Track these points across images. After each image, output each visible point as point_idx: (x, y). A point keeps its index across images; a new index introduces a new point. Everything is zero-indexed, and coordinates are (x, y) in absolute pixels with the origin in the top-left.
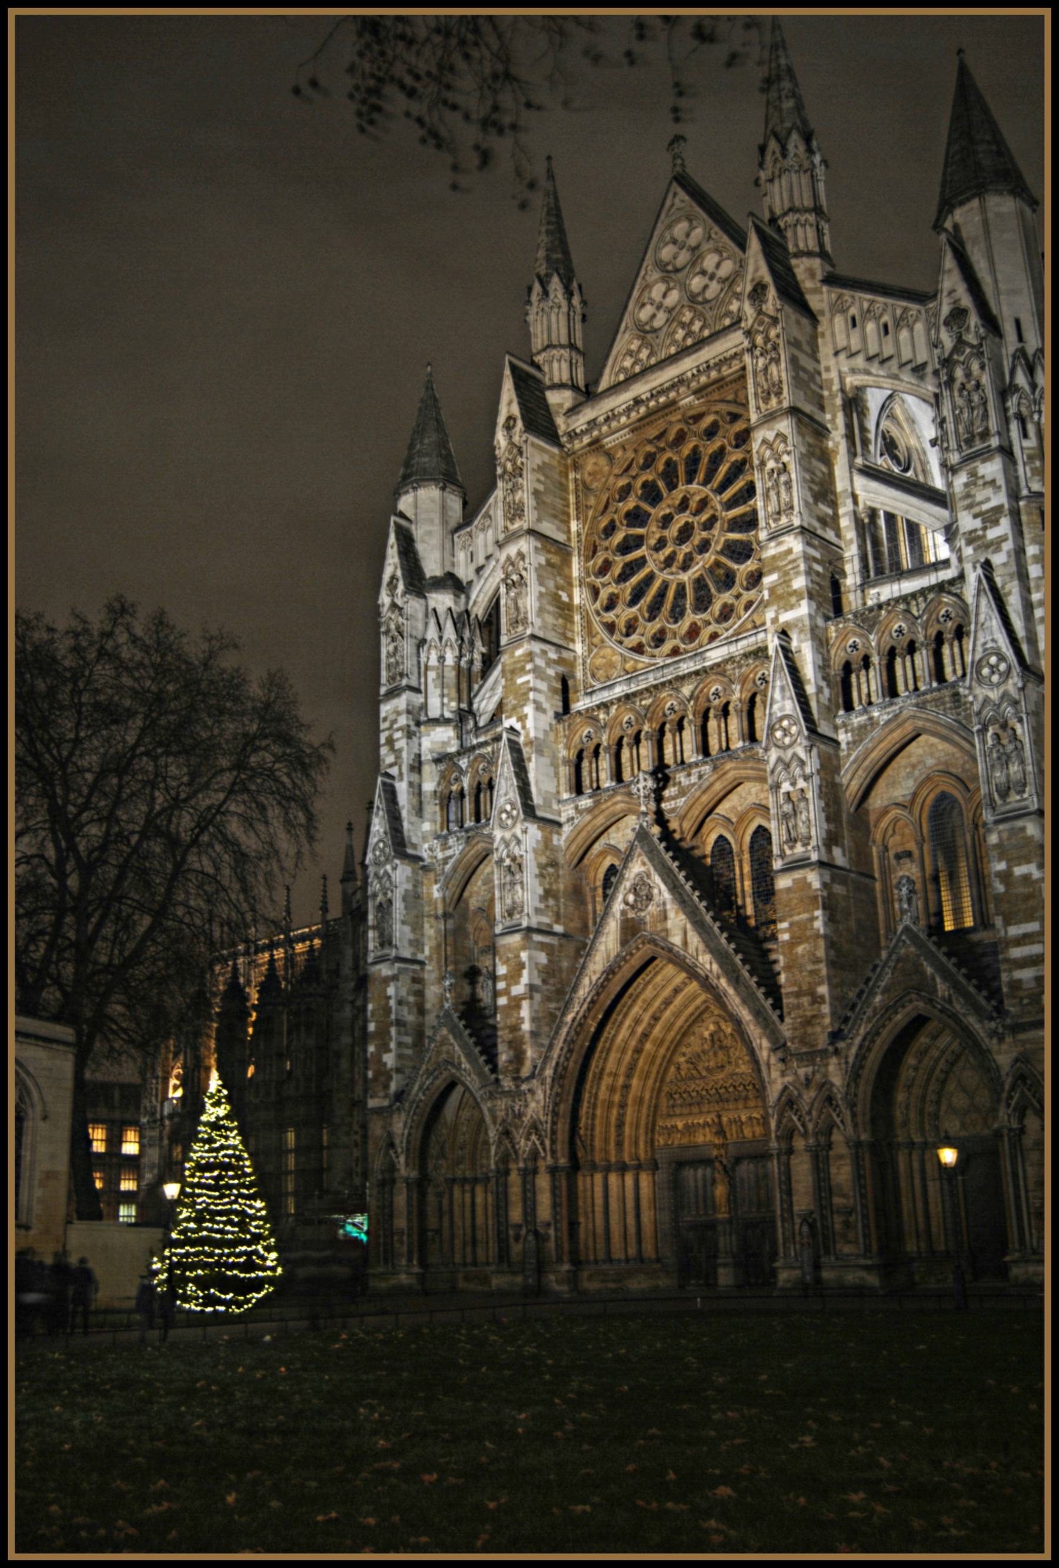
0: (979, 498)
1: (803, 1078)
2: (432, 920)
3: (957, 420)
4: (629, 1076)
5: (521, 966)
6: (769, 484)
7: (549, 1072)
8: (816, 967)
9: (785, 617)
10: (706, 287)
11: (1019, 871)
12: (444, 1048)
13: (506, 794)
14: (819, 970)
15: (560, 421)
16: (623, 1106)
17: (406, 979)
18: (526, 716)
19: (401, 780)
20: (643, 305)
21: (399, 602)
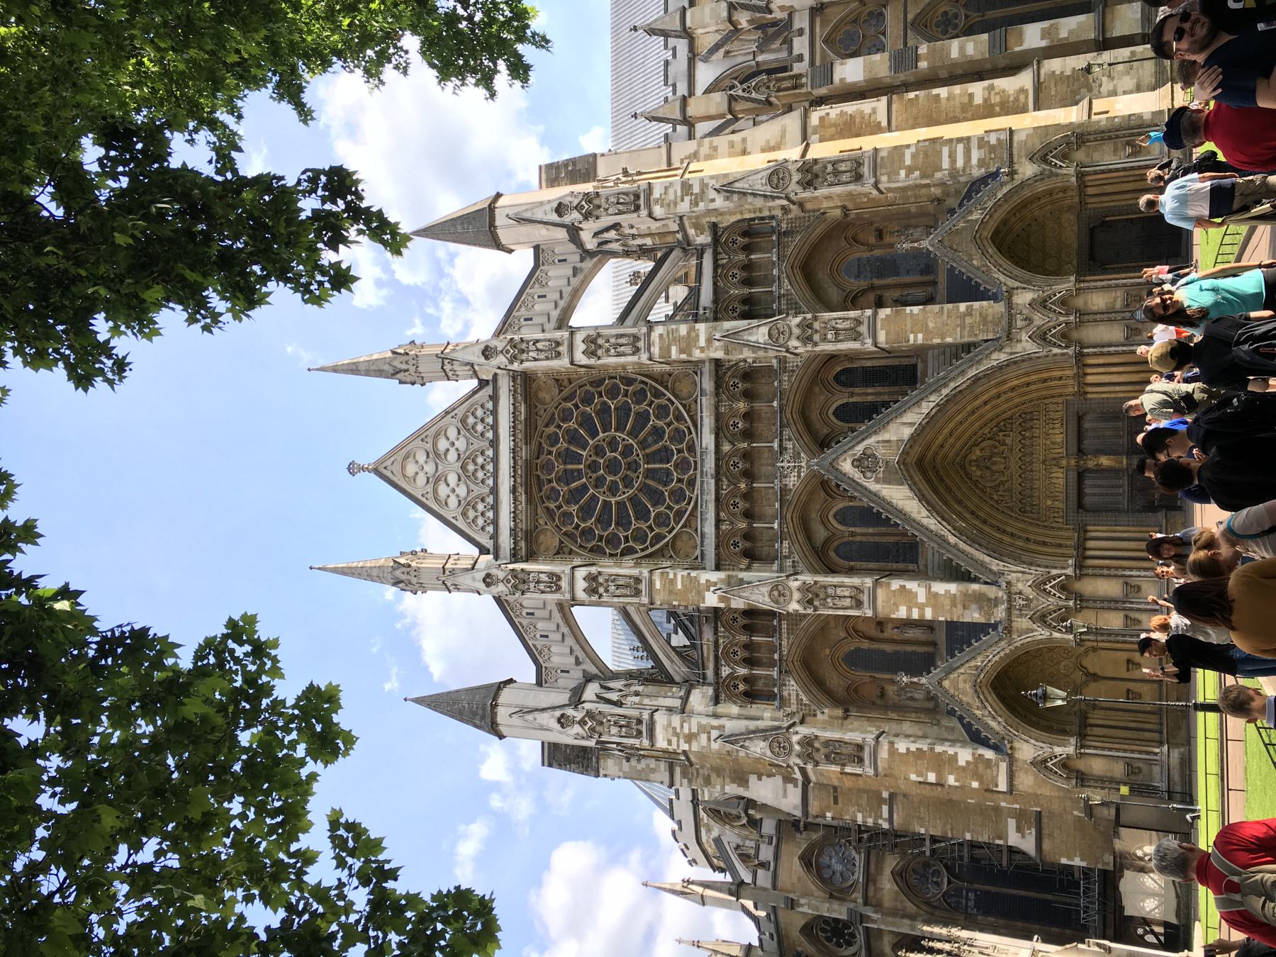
0: (671, 196)
1: (1024, 323)
2: (845, 722)
3: (620, 213)
4: (1004, 532)
6: (613, 351)
7: (995, 565)
8: (946, 311)
9: (702, 343)
10: (457, 450)
11: (908, 161)
12: (961, 685)
17: (896, 740)
18: (708, 581)
20: (446, 503)
21: (579, 715)
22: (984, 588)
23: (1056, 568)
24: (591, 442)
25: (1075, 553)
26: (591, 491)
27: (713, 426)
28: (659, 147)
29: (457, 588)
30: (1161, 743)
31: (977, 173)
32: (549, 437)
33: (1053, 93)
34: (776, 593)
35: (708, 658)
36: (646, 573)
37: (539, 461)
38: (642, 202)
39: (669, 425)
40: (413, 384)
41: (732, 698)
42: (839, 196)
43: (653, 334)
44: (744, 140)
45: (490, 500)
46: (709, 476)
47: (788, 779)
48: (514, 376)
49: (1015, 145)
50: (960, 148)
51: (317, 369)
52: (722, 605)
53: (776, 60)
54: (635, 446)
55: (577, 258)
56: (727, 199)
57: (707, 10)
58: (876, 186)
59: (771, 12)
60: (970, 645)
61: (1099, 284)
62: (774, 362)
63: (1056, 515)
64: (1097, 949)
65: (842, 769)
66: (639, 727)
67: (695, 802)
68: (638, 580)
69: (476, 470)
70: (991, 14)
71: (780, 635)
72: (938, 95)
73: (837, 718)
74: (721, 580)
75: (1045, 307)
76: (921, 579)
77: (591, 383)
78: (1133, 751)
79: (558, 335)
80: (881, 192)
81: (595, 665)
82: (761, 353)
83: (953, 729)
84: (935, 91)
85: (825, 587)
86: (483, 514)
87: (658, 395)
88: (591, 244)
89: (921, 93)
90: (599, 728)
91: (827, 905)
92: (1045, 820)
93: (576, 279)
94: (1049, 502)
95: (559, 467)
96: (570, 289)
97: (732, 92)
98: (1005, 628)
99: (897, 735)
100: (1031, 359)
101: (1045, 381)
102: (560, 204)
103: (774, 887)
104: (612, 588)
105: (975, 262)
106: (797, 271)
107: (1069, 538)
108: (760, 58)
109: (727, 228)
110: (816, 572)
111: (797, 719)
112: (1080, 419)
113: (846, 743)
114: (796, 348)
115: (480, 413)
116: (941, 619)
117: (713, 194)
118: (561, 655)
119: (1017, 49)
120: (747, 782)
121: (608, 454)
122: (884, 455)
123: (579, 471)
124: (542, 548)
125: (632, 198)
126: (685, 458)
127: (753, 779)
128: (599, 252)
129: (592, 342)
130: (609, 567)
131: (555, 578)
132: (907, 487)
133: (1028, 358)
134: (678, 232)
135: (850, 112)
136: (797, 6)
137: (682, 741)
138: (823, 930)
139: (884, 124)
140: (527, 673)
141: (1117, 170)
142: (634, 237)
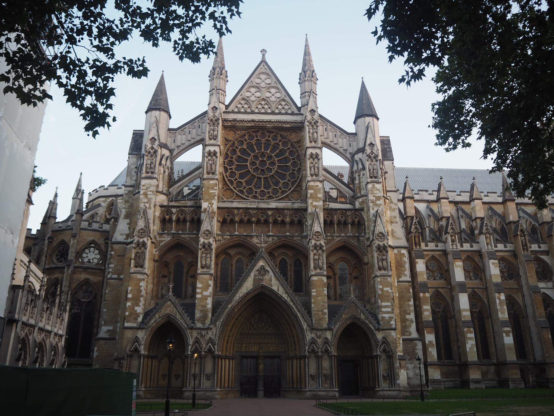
0: (376, 192)
1: (318, 335)
2: (152, 261)
3: (370, 170)
5: (210, 286)
6: (312, 165)
7: (219, 323)
9: (315, 203)
11: (385, 289)
12: (168, 309)
13: (207, 227)
14: (325, 305)
15: (222, 114)
16: (229, 336)
17: (145, 282)
18: (213, 204)
19: (150, 209)
20: (248, 91)
21: (155, 146)
22: (209, 319)
23: (218, 347)
24: (273, 155)
25: (224, 355)
26: (252, 154)
27: (279, 207)
28: (395, 187)
29: (210, 95)
30: (145, 388)
31: (380, 316)
32: (276, 136)
33: (409, 346)
34: (207, 233)
35: (179, 203)
36: (217, 177)
37: (265, 132)
38: (374, 179)
39: (280, 188)
40: (300, 79)
41: (162, 212)
42: (373, 261)
43: (319, 182)
44: (397, 223)
45: (249, 110)
46: (258, 205)
47: (128, 236)
48: (302, 123)
49: (390, 331)
50: (390, 310)
51: (306, 38)
52: (202, 209)
53: (426, 236)
54: (271, 174)
55: (351, 152)
56: (374, 215)
57: (447, 208)
58: (376, 276)
59: (445, 234)
60: (186, 312)
61: (333, 364)
62: (305, 234)
63: (239, 347)
64: (63, 360)
65: (133, 259)
66: (150, 173)
67: (117, 196)
68: (213, 173)
69: (262, 105)
70: (439, 321)
71: (190, 234)
72: (410, 301)
73: (154, 257)
74: (213, 210)
75: (325, 343)
76: (213, 293)
77: (298, 155)
78: (142, 376)
79: (319, 142)
80: (374, 278)
81: (177, 154)
82: (309, 228)
83: (150, 305)
84: (412, 300)
85: (210, 253)
86: (243, 107)
87: (293, 184)
88: (357, 157)
89: (411, 294)
90: (149, 155)
91: (74, 251)
92: (112, 341)
93: (342, 151)
94: (244, 345)
95: (263, 141)
96: (338, 148)
97: (415, 218)
98: (193, 327)
99: (147, 282)
100: (304, 338)
101: (294, 343)
102: (374, 145)
103: (81, 229)
104: (210, 162)
105: (344, 316)
106: (343, 244)
107: (229, 353)
108: (427, 229)
109: (362, 215)
110: (216, 250)
111: (153, 240)
112: (279, 357)
113: (144, 260)
114: (311, 243)
115: (286, 107)
116: (196, 301)
117: (376, 209)
118: (181, 140)
119: (425, 331)
120: (126, 219)
121: (268, 162)
122: (266, 279)
123: (261, 149)
124: (227, 132)
125: (375, 175)
126: (266, 195)
127: (128, 221)
128: (353, 161)
129: (316, 156)
130: (219, 161)
131: (215, 138)
132: (252, 288)
133: (304, 337)
134: (361, 194)
135: (406, 266)
136: (447, 244)
137: (144, 191)
138: (63, 249)
139: (400, 279)
140: (174, 124)
141: (378, 371)
142: (359, 176)
